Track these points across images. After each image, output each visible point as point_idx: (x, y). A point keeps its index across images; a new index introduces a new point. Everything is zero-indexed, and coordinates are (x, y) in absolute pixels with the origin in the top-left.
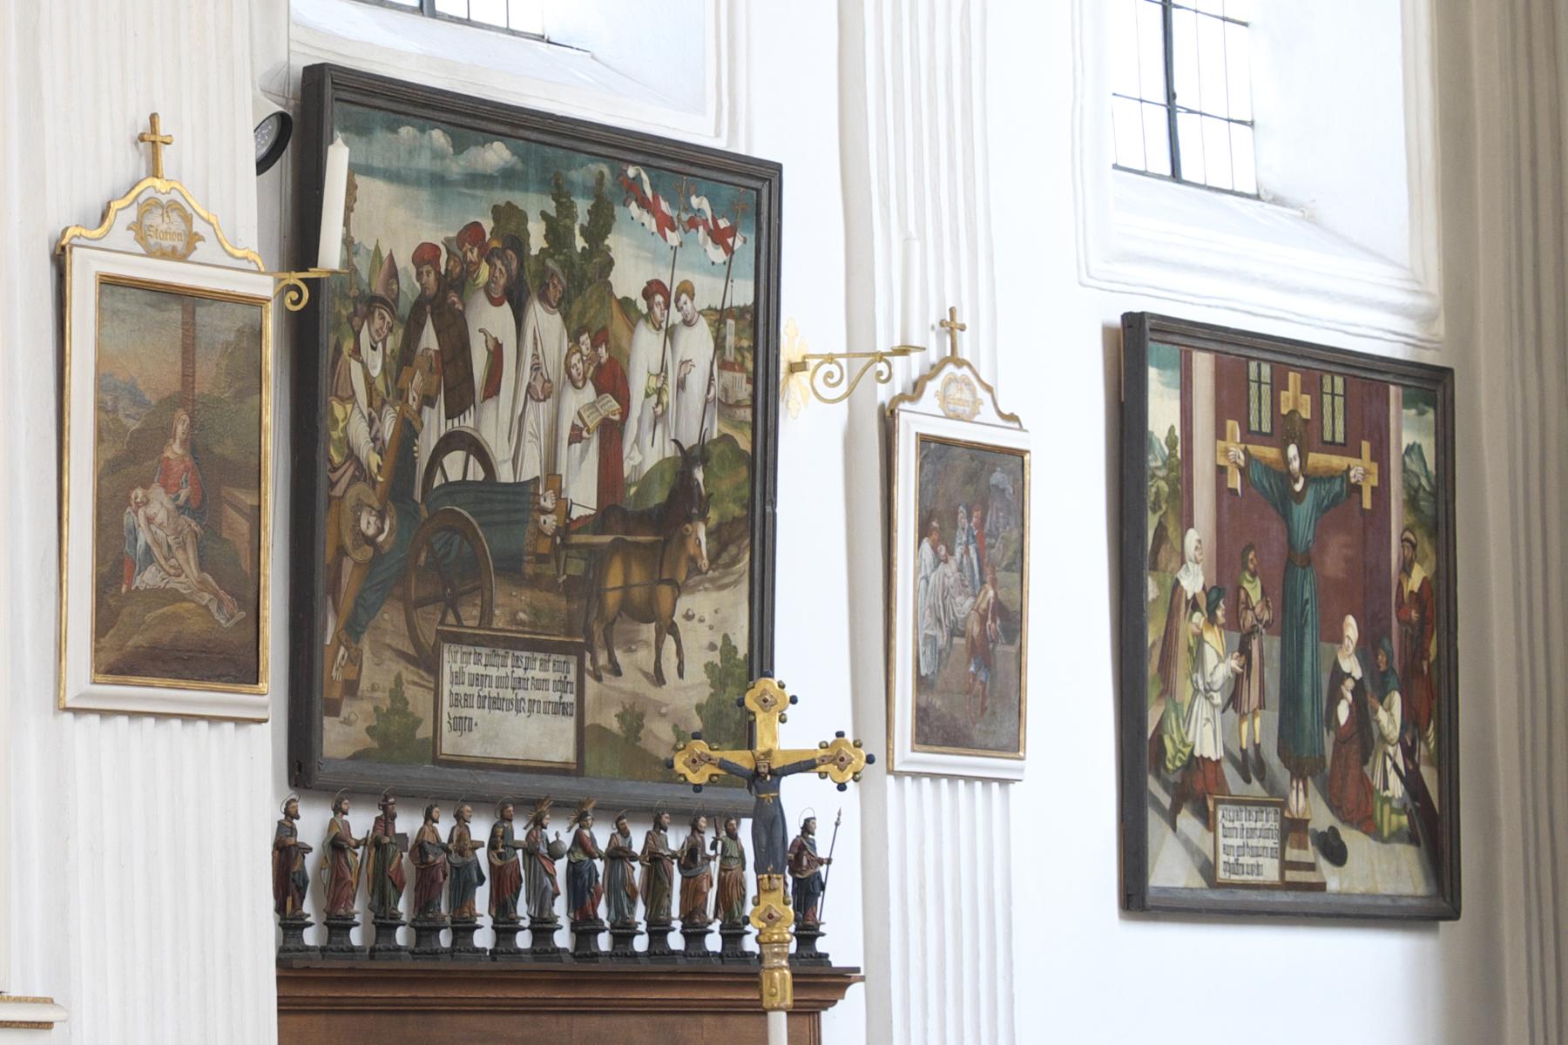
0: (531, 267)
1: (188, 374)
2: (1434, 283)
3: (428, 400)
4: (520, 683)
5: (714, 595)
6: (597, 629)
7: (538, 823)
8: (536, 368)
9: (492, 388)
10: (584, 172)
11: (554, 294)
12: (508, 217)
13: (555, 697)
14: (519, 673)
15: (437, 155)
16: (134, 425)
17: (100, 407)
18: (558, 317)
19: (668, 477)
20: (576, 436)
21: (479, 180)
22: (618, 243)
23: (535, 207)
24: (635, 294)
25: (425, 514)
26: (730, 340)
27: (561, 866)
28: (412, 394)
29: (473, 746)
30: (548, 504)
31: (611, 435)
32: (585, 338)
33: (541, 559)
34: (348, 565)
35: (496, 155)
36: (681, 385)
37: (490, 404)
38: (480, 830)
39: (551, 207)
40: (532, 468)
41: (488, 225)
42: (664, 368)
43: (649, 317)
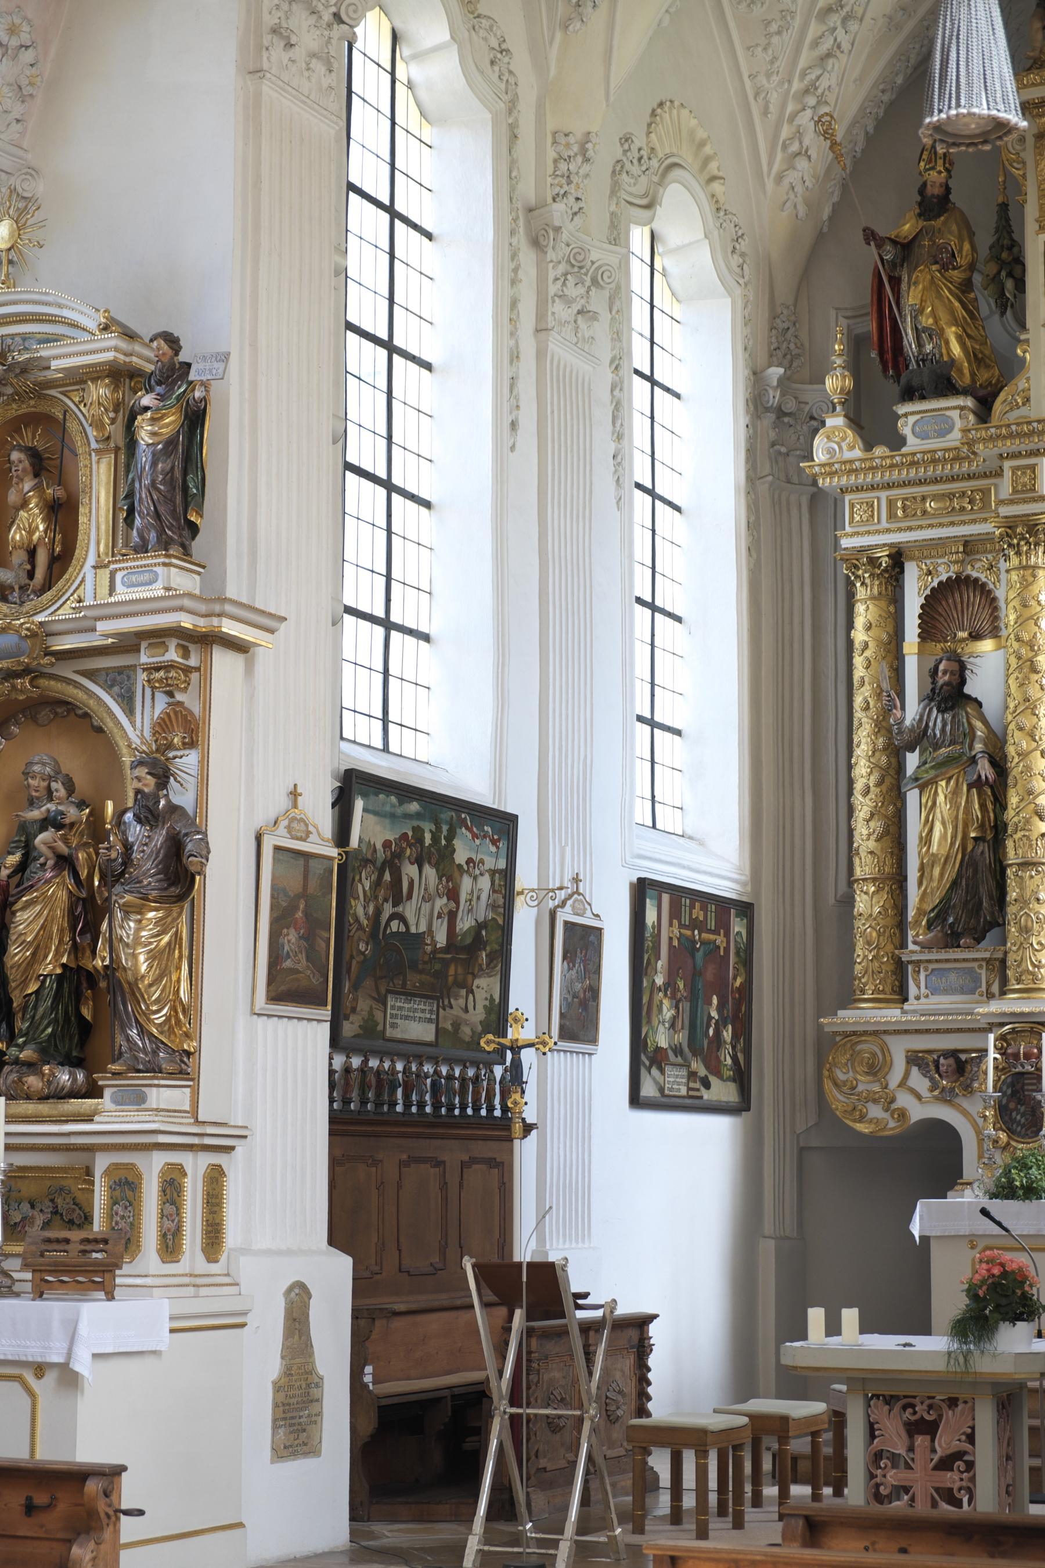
0: (425, 850)
1: (305, 886)
2: (748, 872)
3: (386, 900)
4: (415, 1010)
5: (488, 979)
6: (445, 992)
7: (421, 1064)
8: (426, 889)
9: (410, 896)
10: (446, 815)
11: (433, 861)
12: (418, 831)
13: (428, 1016)
15: (393, 806)
19: (473, 933)
20: (439, 917)
21: (407, 816)
22: (457, 843)
23: (428, 827)
24: (463, 863)
25: (383, 943)
26: (497, 882)
27: (429, 1081)
28: (380, 898)
29: (398, 1034)
30: (429, 942)
31: (452, 916)
33: (425, 963)
34: (354, 963)
35: (414, 807)
36: (478, 898)
37: (408, 903)
38: (399, 1067)
39: (433, 828)
40: (423, 928)
41: (410, 834)
42: (472, 891)
43: (467, 872)
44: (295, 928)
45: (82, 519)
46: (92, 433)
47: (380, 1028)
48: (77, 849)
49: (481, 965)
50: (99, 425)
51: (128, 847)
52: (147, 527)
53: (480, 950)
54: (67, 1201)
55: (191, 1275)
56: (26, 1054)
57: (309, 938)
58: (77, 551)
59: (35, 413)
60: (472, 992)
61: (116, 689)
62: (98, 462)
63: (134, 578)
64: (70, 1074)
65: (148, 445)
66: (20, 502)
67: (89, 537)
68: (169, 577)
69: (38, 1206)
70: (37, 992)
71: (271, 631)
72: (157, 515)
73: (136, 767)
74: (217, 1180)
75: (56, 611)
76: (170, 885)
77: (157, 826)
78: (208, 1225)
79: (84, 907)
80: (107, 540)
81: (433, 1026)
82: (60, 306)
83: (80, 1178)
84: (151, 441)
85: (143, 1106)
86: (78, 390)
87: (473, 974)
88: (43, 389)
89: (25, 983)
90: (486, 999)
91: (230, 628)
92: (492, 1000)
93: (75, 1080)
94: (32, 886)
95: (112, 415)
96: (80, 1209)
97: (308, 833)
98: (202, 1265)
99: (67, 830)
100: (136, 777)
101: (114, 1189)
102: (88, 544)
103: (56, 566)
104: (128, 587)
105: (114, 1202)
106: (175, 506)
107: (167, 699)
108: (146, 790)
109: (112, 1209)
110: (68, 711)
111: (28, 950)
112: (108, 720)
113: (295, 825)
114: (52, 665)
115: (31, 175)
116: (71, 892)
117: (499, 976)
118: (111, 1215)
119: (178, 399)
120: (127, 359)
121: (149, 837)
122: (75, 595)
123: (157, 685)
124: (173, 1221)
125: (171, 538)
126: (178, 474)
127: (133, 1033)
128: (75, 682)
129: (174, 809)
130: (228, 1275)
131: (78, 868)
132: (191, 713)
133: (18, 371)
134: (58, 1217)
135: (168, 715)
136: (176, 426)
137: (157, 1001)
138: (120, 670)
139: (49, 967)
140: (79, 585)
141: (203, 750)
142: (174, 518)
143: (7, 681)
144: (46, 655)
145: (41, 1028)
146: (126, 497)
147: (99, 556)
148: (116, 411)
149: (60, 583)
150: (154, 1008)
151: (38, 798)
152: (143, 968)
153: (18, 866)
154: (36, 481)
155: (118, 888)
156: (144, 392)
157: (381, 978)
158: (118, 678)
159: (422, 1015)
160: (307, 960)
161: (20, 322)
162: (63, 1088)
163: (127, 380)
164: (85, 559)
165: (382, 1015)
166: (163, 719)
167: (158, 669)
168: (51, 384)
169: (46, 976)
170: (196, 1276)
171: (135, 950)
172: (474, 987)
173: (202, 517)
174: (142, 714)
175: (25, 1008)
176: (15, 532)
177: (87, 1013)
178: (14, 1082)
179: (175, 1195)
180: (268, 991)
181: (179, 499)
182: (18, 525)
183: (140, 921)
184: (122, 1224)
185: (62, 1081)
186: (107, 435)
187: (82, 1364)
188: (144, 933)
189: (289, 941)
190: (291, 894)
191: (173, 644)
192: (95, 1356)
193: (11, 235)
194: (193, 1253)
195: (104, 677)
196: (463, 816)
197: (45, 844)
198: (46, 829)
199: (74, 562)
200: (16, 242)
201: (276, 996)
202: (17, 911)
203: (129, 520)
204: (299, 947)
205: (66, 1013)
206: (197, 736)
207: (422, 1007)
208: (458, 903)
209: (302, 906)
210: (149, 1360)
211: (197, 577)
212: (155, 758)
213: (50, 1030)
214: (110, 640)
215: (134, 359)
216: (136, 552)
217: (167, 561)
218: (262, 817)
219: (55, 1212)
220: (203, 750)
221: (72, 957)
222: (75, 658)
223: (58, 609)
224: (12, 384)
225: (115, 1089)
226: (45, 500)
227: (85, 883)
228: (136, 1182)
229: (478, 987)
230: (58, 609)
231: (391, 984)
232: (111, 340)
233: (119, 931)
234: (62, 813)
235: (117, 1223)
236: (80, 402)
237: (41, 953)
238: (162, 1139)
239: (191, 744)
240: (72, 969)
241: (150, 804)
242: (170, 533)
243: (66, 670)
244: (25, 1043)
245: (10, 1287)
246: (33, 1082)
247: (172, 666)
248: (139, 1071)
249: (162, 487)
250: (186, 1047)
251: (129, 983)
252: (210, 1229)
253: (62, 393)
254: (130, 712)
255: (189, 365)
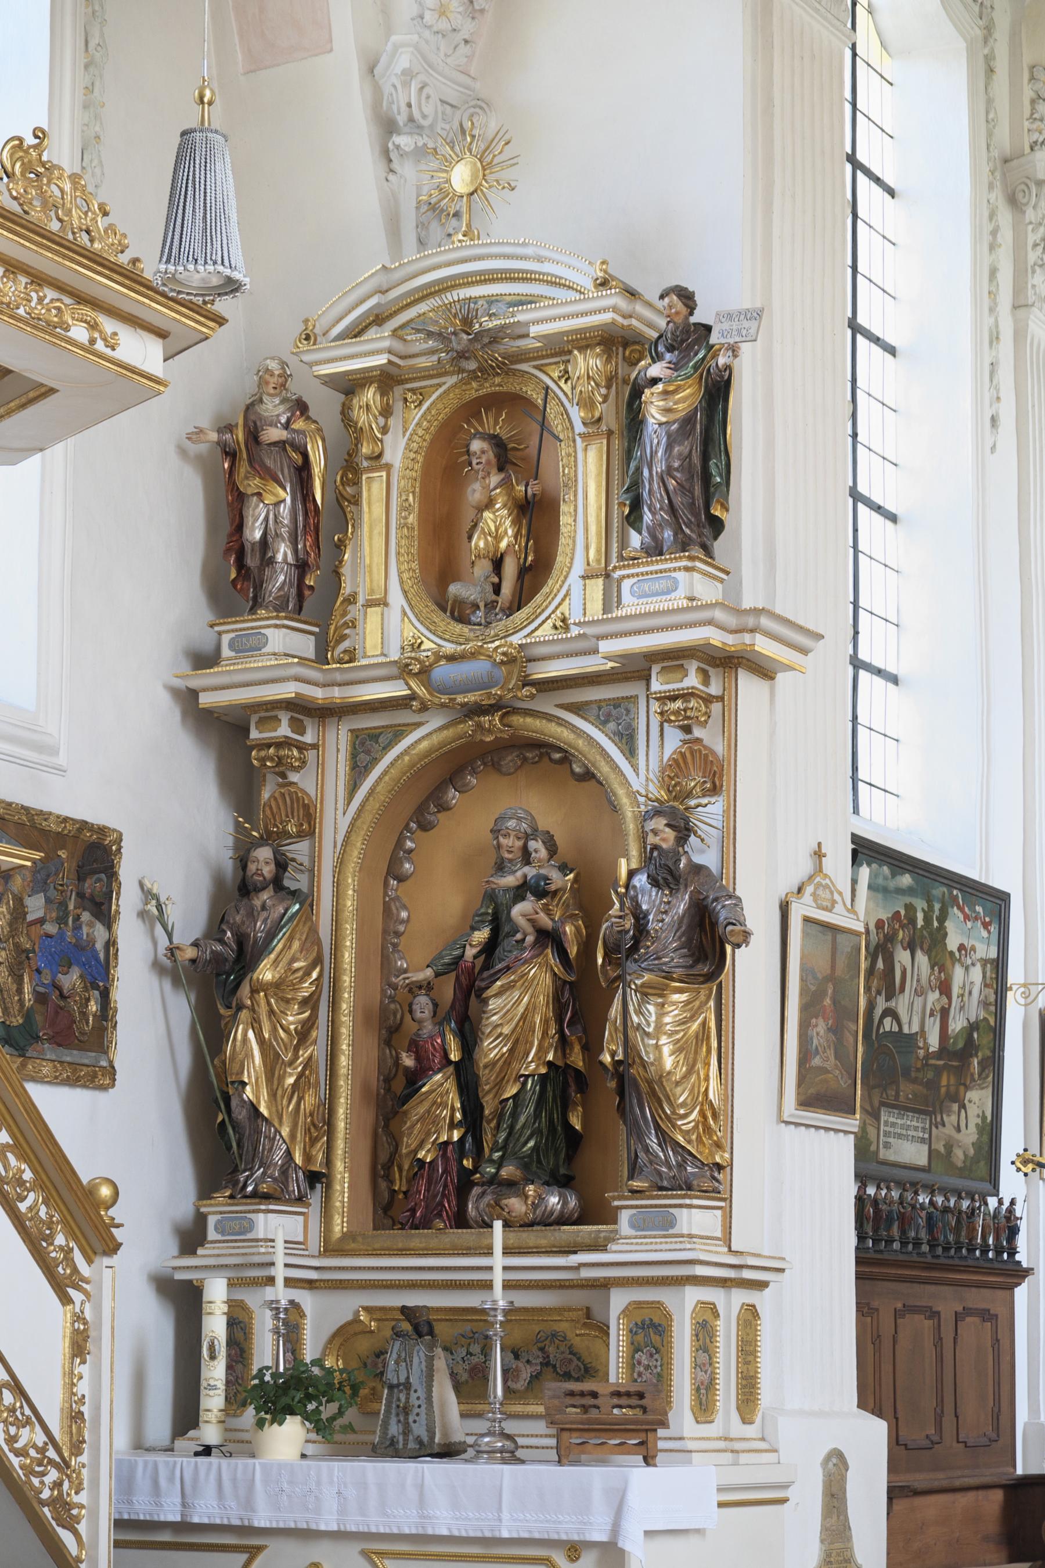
0: (918, 933)
3: (879, 993)
4: (908, 1128)
6: (938, 1107)
7: (916, 1193)
8: (918, 981)
9: (902, 990)
10: (939, 891)
11: (925, 946)
12: (910, 908)
13: (921, 1135)
14: (909, 1123)
15: (885, 878)
16: (813, 988)
17: (802, 980)
18: (926, 958)
19: (964, 1036)
20: (932, 1015)
21: (899, 891)
22: (949, 925)
24: (955, 950)
26: (988, 974)
27: (923, 1214)
28: (873, 989)
29: (890, 1155)
30: (921, 1045)
31: (945, 1013)
32: (936, 968)
33: (918, 1070)
36: (970, 993)
37: (901, 996)
40: (915, 1028)
41: (903, 912)
42: (964, 985)
43: (959, 960)
44: (823, 1018)
45: (564, 520)
46: (577, 415)
47: (873, 1148)
48: (562, 923)
49: (972, 1075)
50: (586, 403)
51: (640, 918)
52: (660, 525)
53: (971, 1056)
54: (562, 1349)
55: (726, 1439)
56: (508, 1171)
57: (836, 1030)
58: (559, 559)
59: (500, 393)
60: (964, 1107)
61: (612, 725)
62: (586, 450)
63: (646, 587)
64: (561, 1196)
65: (660, 424)
66: (486, 501)
67: (574, 541)
68: (691, 586)
69: (524, 1357)
70: (515, 1097)
71: (804, 651)
72: (672, 509)
73: (651, 819)
74: (750, 1324)
75: (533, 632)
76: (696, 962)
77: (678, 890)
78: (742, 1378)
79: (571, 989)
80: (599, 543)
81: (926, 1147)
82: (540, 259)
83: (578, 1322)
84: (664, 420)
85: (671, 1232)
86: (556, 363)
87: (965, 1085)
88: (512, 363)
89: (500, 1085)
90: (978, 1116)
91: (764, 646)
92: (984, 1118)
93: (565, 1203)
94: (508, 968)
95: (603, 391)
96: (579, 1359)
97: (834, 902)
98: (737, 1428)
99: (549, 898)
100: (652, 830)
101: (636, 1333)
102: (574, 549)
103: (527, 578)
104: (639, 597)
105: (635, 1348)
106: (693, 498)
107: (680, 735)
108: (664, 846)
109: (633, 1357)
110: (541, 756)
111: (505, 1045)
112: (603, 763)
113: (820, 892)
114: (532, 697)
115: (481, 108)
116: (555, 974)
117: (990, 1089)
118: (632, 1364)
119: (696, 368)
120: (626, 322)
121: (669, 903)
122: (558, 612)
123: (673, 718)
124: (706, 1372)
125: (689, 538)
126: (696, 459)
127: (653, 1142)
128: (559, 718)
129: (698, 869)
130: (763, 1439)
131: (566, 945)
132: (713, 753)
133: (486, 340)
134: (550, 1369)
135: (683, 755)
136: (696, 400)
137: (683, 1105)
138: (616, 703)
139: (531, 1066)
140: (563, 600)
141: (729, 796)
142: (692, 514)
143: (471, 719)
144: (524, 686)
145: (522, 1140)
146: (628, 490)
147: (588, 564)
148: (608, 387)
149: (538, 598)
150: (682, 1111)
151: (510, 861)
152: (668, 1062)
153: (486, 944)
154: (502, 476)
155: (631, 966)
156: (650, 361)
157: (874, 1087)
158: (614, 712)
159: (914, 1133)
160: (836, 1058)
161: (485, 281)
162: (552, 1213)
163: (621, 349)
164: (570, 568)
165: (876, 1132)
166: (675, 761)
167: (673, 698)
168: (523, 356)
169: (527, 1077)
170: (732, 1440)
171: (658, 1040)
172: (966, 1102)
173: (727, 510)
174: (647, 755)
175: (500, 1116)
176: (479, 538)
177: (577, 1124)
178: (489, 1205)
179: (708, 1340)
180: (798, 1094)
181: (698, 490)
182: (483, 529)
183: (663, 1005)
184: (646, 1376)
185: (551, 1204)
186: (597, 415)
187: (633, 1543)
188: (667, 1019)
189: (818, 1034)
190: (820, 976)
191: (693, 666)
192: (648, 1534)
193: (474, 176)
194: (727, 1413)
195: (595, 711)
196: (955, 892)
197: (524, 916)
198: (523, 899)
199: (555, 572)
200: (481, 184)
201: (808, 1101)
202: (489, 998)
203: (633, 518)
204: (828, 1041)
205: (551, 1121)
206: (721, 780)
207: (914, 1123)
208: (950, 998)
209: (830, 991)
210: (694, 1540)
211: (719, 585)
212: (673, 807)
213: (531, 1144)
214: (611, 664)
215: (634, 322)
216: (649, 555)
217: (689, 564)
218: (785, 884)
219: (546, 1364)
220: (729, 796)
221: (559, 1053)
222: (558, 689)
223: (536, 629)
224: (476, 357)
225: (634, 1211)
226: (515, 499)
227: (574, 963)
228: (664, 1323)
229: (970, 1101)
230: (536, 629)
231: (884, 1095)
232: (613, 298)
233: (635, 1019)
234: (546, 878)
235: (640, 1374)
236: (560, 378)
237: (521, 1048)
238: (700, 1271)
239: (715, 790)
240: (557, 1067)
241: (670, 864)
242: (687, 531)
243: (547, 704)
244: (502, 1157)
245: (512, 1452)
246: (516, 1205)
247: (692, 694)
248: (661, 1188)
249: (678, 475)
250: (718, 1159)
251: (649, 1082)
252: (744, 1382)
253: (536, 367)
254: (630, 752)
255: (708, 329)
